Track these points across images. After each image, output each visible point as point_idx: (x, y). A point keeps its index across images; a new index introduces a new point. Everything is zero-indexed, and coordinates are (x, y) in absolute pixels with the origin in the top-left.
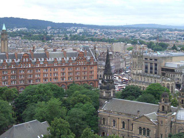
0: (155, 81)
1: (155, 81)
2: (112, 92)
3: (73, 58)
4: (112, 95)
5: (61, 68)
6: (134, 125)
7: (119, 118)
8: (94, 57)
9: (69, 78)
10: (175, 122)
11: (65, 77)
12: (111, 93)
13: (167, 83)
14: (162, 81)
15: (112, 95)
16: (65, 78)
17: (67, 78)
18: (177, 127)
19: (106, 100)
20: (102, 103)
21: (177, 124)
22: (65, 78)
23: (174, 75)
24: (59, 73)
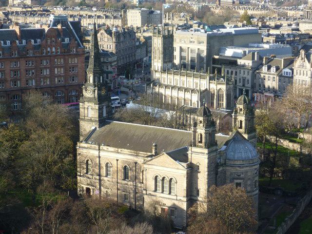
0: (197, 84)
1: (197, 84)
2: (105, 107)
3: (36, 42)
4: (105, 115)
5: (11, 62)
6: (144, 172)
7: (117, 160)
8: (79, 40)
9: (27, 81)
10: (225, 164)
11: (20, 80)
12: (103, 111)
13: (219, 87)
14: (209, 83)
15: (105, 115)
16: (19, 82)
17: (24, 80)
18: (228, 173)
19: (94, 123)
20: (85, 130)
21: (228, 168)
22: (19, 82)
23: (236, 72)
24: (7, 71)
